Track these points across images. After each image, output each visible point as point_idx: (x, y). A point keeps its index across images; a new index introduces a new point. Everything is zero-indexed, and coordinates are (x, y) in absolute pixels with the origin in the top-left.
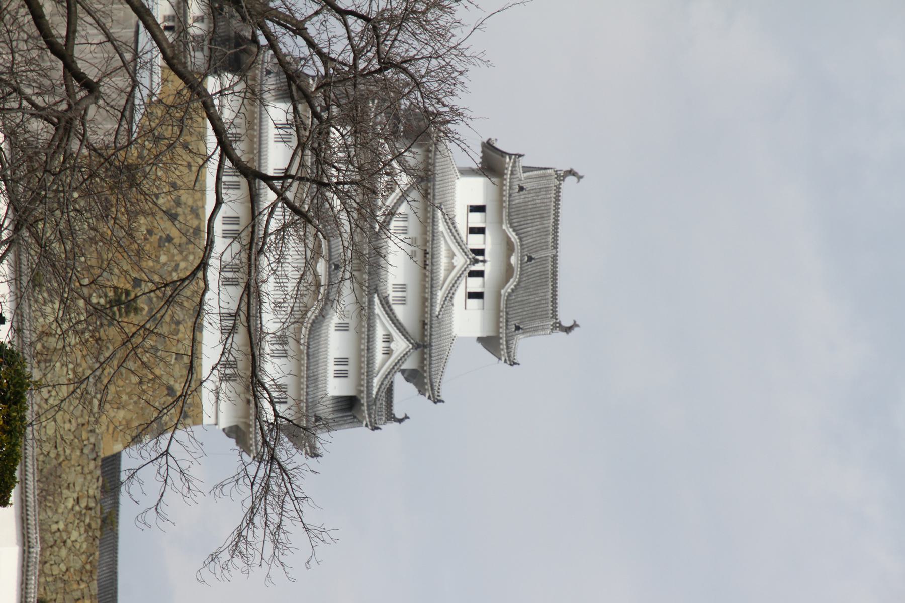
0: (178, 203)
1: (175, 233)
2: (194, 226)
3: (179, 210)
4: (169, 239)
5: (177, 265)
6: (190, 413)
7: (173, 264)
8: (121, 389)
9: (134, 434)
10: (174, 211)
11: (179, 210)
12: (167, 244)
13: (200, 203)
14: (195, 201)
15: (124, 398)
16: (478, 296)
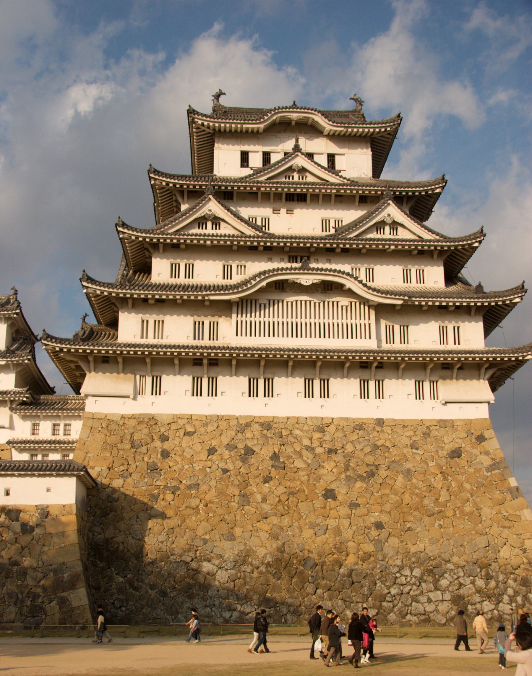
0: (230, 447)
1: (266, 452)
2: (260, 429)
3: (241, 446)
4: (275, 457)
5: (307, 448)
6: (479, 434)
7: (305, 453)
8: (457, 512)
9: (509, 497)
10: (243, 452)
11: (241, 446)
12: (282, 460)
13: (234, 423)
14: (229, 428)
15: (468, 508)
16: (331, 158)
